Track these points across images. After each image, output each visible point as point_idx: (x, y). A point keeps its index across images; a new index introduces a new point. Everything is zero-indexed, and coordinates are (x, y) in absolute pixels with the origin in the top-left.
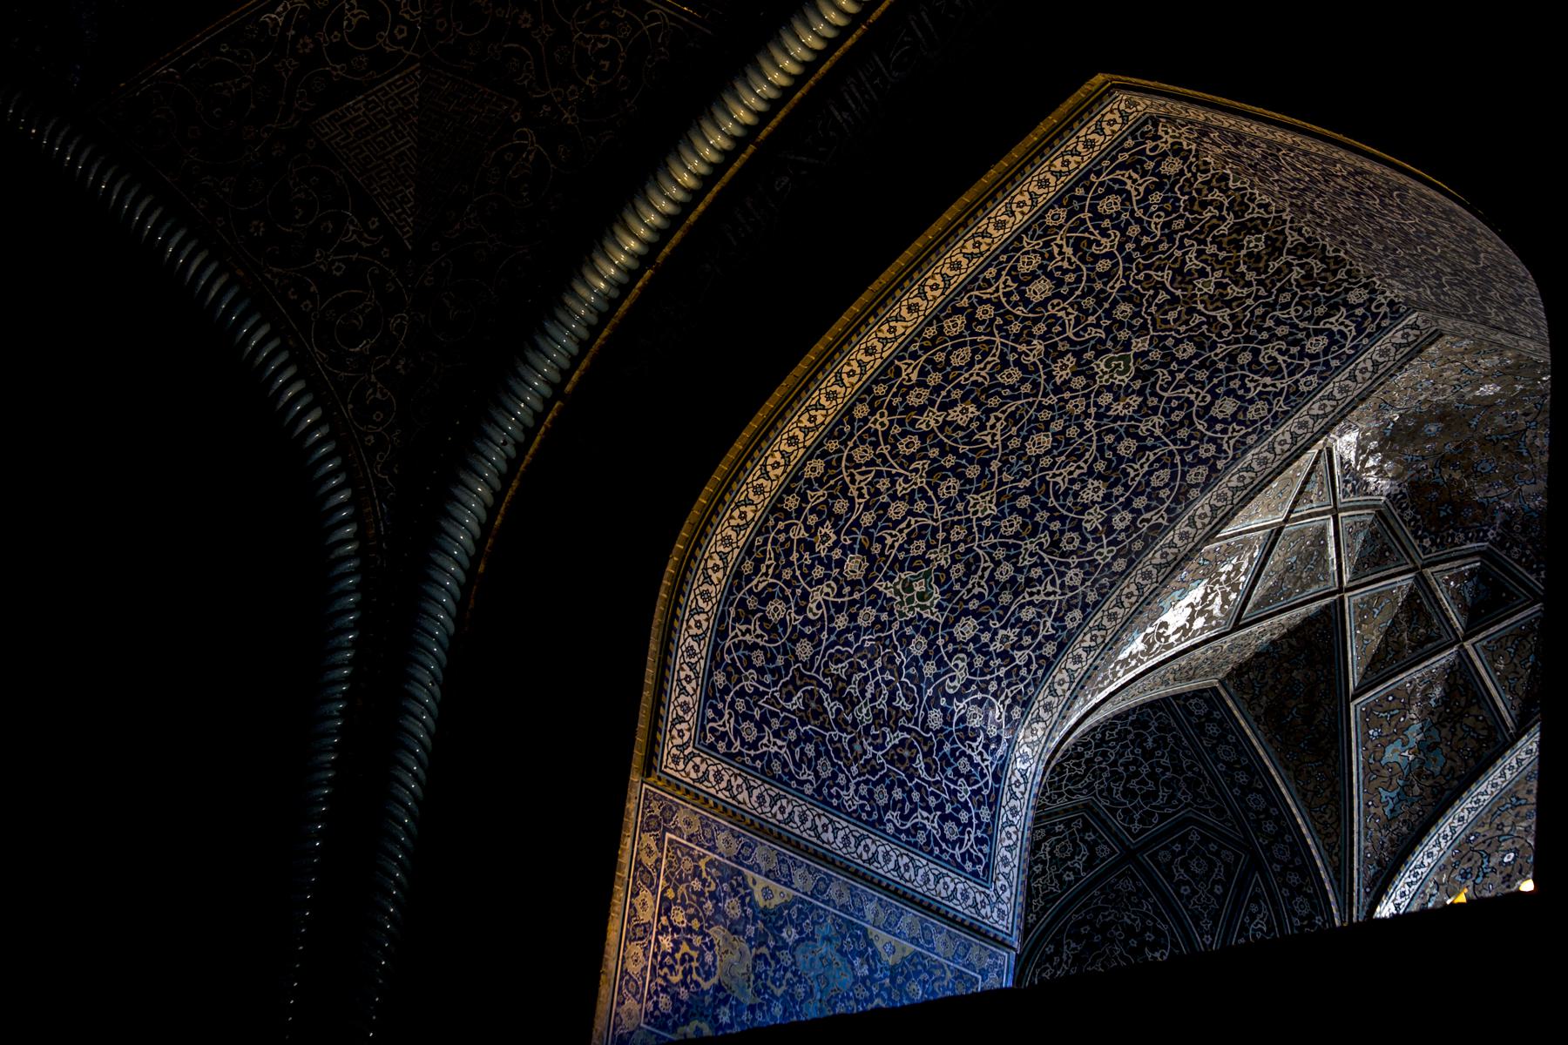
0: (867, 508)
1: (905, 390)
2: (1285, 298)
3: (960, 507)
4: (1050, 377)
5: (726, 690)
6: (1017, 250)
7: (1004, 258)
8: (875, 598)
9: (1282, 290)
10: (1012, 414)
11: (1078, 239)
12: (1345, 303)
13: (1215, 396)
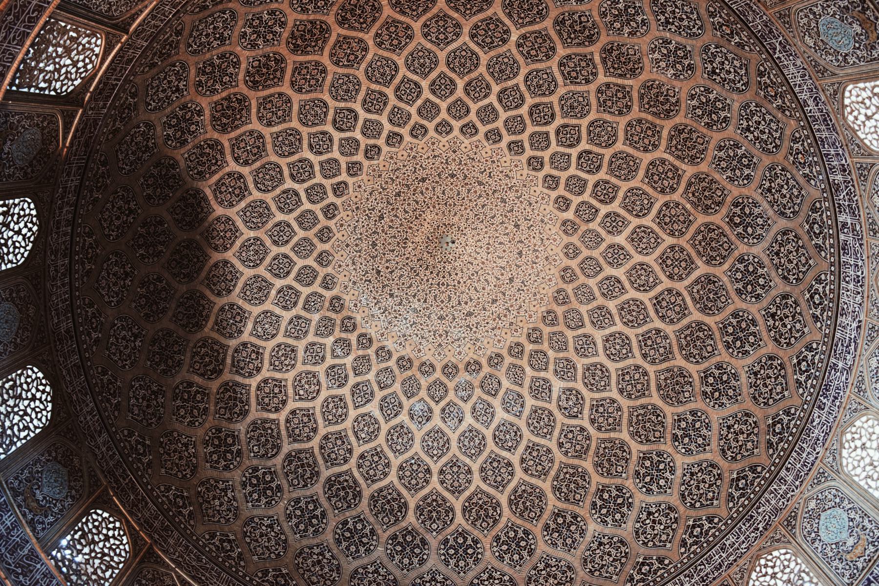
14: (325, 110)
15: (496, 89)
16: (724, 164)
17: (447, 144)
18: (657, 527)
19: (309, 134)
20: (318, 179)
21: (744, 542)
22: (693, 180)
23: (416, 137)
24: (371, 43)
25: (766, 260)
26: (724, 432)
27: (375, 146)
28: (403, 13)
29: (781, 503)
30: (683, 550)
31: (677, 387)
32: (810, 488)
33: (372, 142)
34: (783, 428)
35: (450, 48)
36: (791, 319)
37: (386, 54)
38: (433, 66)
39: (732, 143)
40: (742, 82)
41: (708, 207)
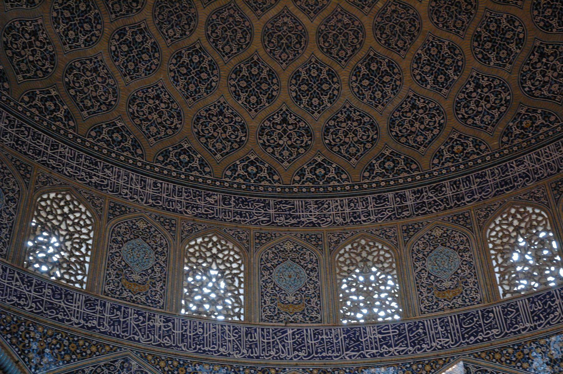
16: (434, 51)
18: (28, 51)
21: (72, 167)
22: (411, 12)
25: (338, 104)
26: (152, 94)
29: (125, 191)
30: (26, 99)
31: (174, 17)
32: (153, 216)
34: (187, 163)
36: (289, 143)
39: (460, 63)
40: (533, 88)
41: (382, 29)
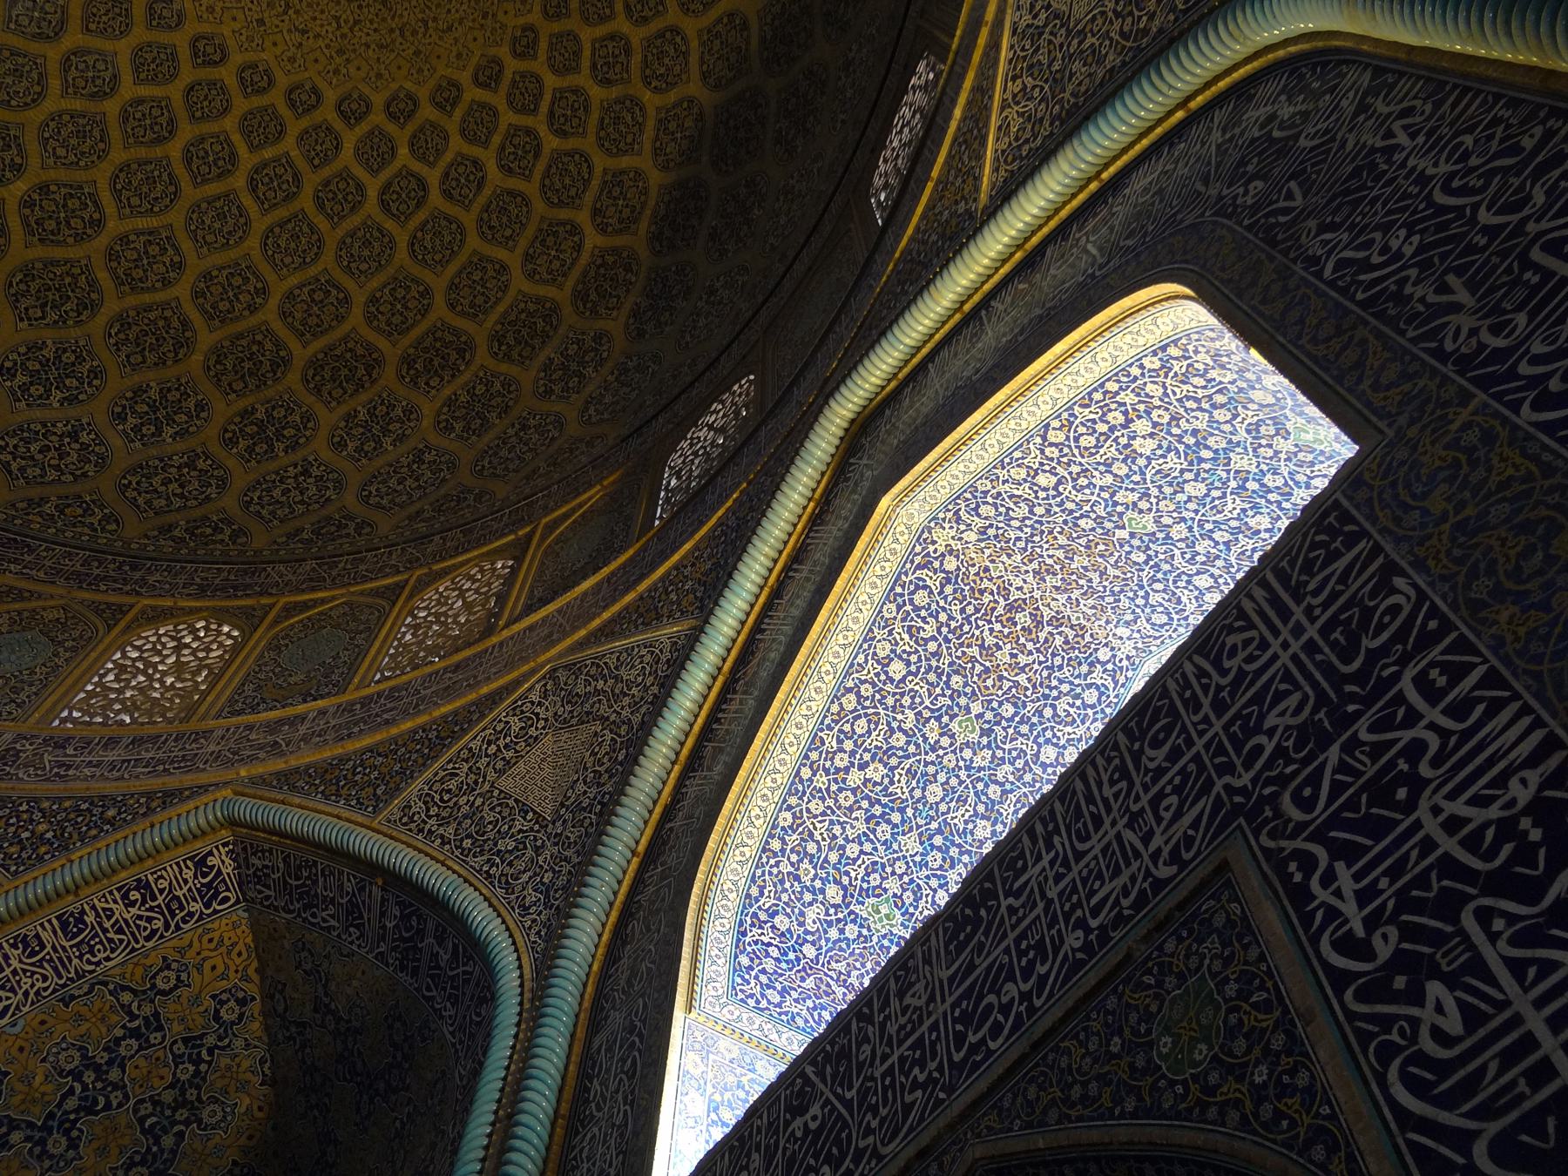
0: (830, 849)
1: (831, 756)
2: (1057, 661)
3: (895, 846)
4: (925, 739)
5: (750, 968)
6: (873, 639)
7: (865, 646)
8: (855, 918)
9: (1054, 655)
10: (909, 770)
11: (910, 627)
12: (1098, 661)
13: (1039, 746)
14: (419, 234)
15: (112, 107)
17: (268, 44)
19: (467, 208)
20: (508, 118)
23: (315, 91)
24: (274, 302)
27: (392, 116)
28: (185, 324)
33: (391, 128)
35: (153, 222)
37: (265, 269)
38: (204, 205)
